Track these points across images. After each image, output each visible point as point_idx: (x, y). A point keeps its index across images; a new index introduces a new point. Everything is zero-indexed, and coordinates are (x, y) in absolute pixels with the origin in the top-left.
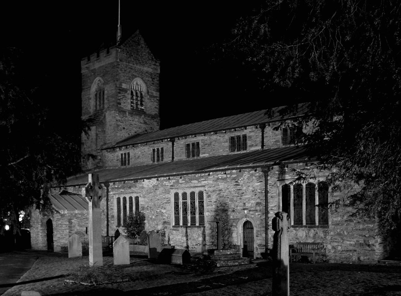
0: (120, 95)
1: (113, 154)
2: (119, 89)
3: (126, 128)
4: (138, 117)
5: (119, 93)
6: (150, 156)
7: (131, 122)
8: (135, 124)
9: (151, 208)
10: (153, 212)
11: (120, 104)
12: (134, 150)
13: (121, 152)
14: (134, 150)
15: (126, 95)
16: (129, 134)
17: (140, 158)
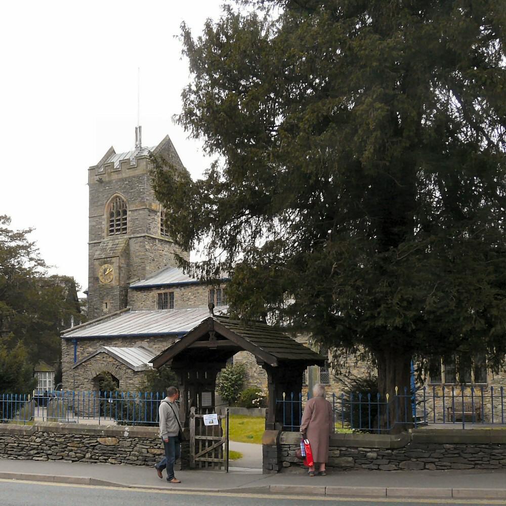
0: (149, 218)
1: (145, 294)
2: (149, 211)
3: (155, 260)
4: (168, 246)
5: (149, 216)
6: (207, 298)
7: (161, 252)
8: (166, 255)
9: (251, 363)
10: (254, 369)
11: (150, 230)
12: (181, 290)
13: (159, 292)
14: (181, 290)
15: (156, 218)
16: (158, 267)
17: (190, 300)
